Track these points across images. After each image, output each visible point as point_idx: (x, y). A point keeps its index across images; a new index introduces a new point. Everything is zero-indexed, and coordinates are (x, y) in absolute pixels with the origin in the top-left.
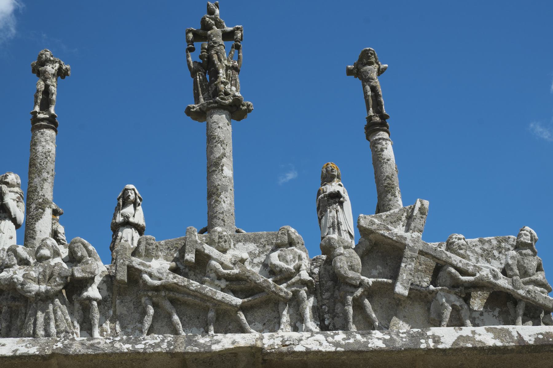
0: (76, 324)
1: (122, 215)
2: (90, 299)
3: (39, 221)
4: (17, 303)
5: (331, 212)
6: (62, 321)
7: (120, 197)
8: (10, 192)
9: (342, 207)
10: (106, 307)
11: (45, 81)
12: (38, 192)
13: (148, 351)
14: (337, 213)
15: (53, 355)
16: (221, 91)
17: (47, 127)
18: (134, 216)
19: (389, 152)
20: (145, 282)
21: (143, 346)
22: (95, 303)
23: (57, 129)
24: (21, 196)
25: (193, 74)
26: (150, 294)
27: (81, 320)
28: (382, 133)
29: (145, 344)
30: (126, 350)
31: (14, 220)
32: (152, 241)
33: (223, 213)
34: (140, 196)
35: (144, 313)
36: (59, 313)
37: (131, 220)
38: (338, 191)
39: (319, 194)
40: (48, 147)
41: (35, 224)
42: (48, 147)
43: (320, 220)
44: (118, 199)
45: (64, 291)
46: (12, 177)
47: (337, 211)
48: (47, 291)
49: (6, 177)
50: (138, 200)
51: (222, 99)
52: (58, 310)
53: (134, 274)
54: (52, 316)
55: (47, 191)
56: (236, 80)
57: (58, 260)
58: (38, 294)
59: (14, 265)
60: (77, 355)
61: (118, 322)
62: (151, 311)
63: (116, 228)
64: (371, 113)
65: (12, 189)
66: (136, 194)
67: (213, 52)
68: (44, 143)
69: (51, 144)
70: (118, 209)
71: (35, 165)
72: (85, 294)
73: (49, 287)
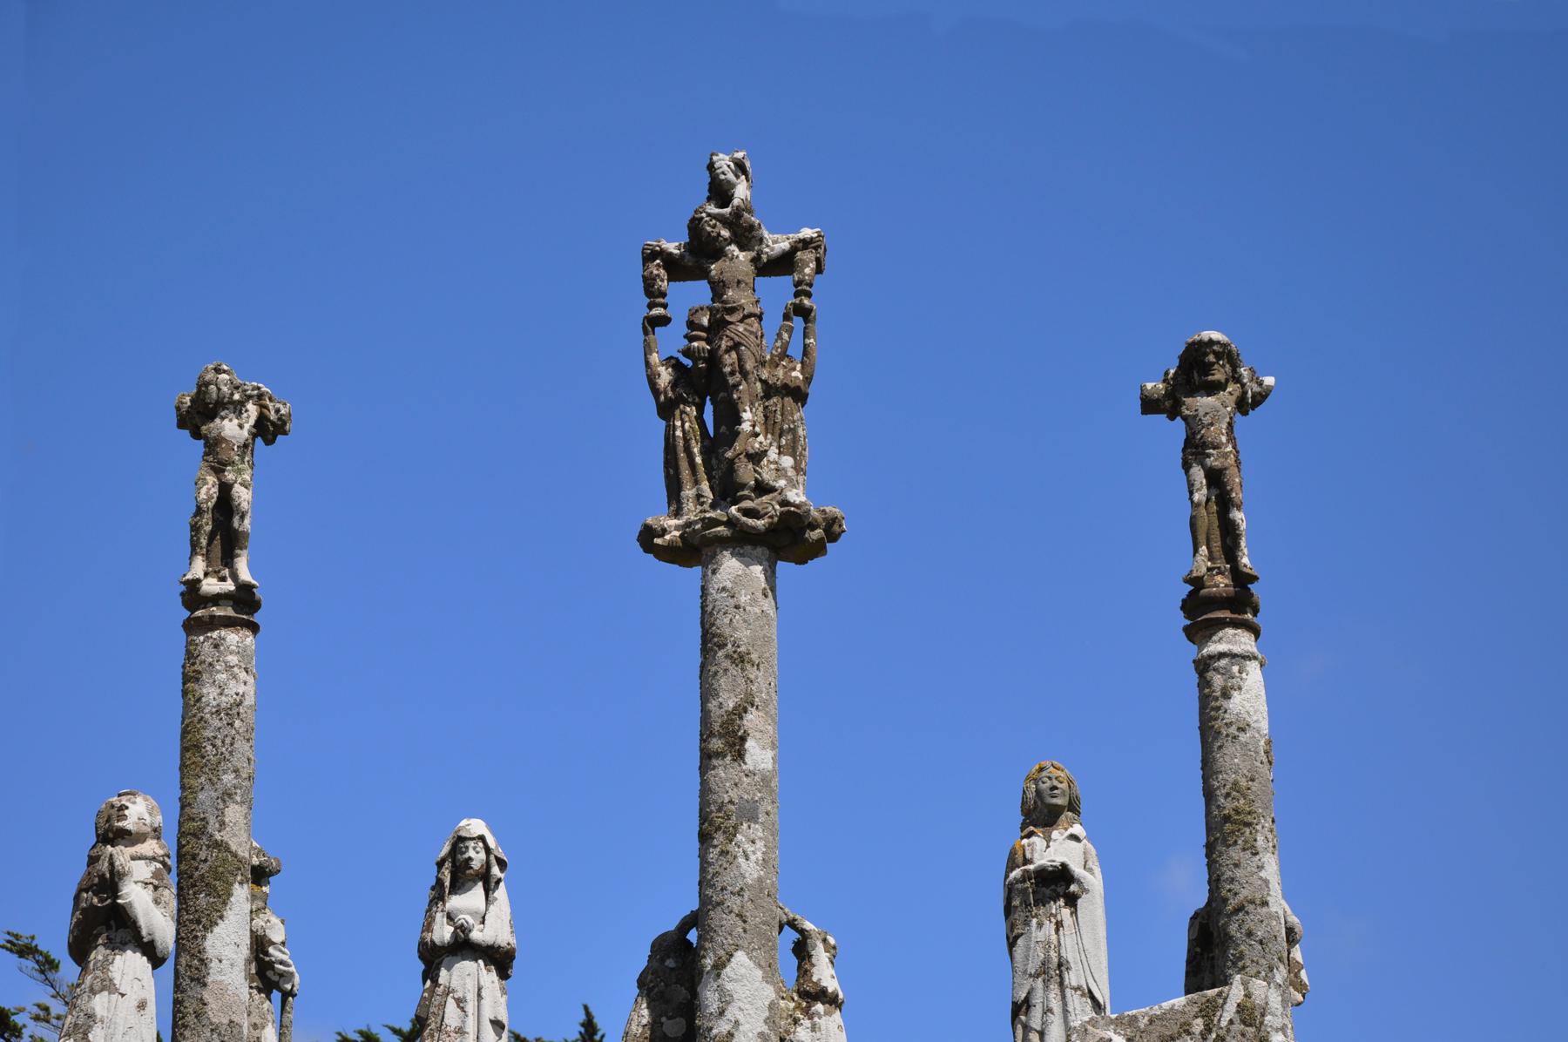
3: (216, 930)
5: (1040, 925)
8: (133, 858)
9: (1074, 913)
11: (218, 470)
14: (1057, 931)
16: (743, 486)
17: (229, 623)
19: (1250, 698)
23: (257, 618)
25: (666, 410)
28: (1230, 631)
33: (740, 893)
37: (476, 935)
38: (1063, 865)
39: (1012, 865)
40: (234, 688)
41: (204, 937)
43: (1012, 944)
47: (1059, 925)
50: (495, 870)
51: (748, 513)
56: (793, 431)
63: (433, 958)
64: (1202, 564)
66: (488, 850)
67: (724, 344)
68: (222, 677)
69: (243, 675)
71: (197, 747)
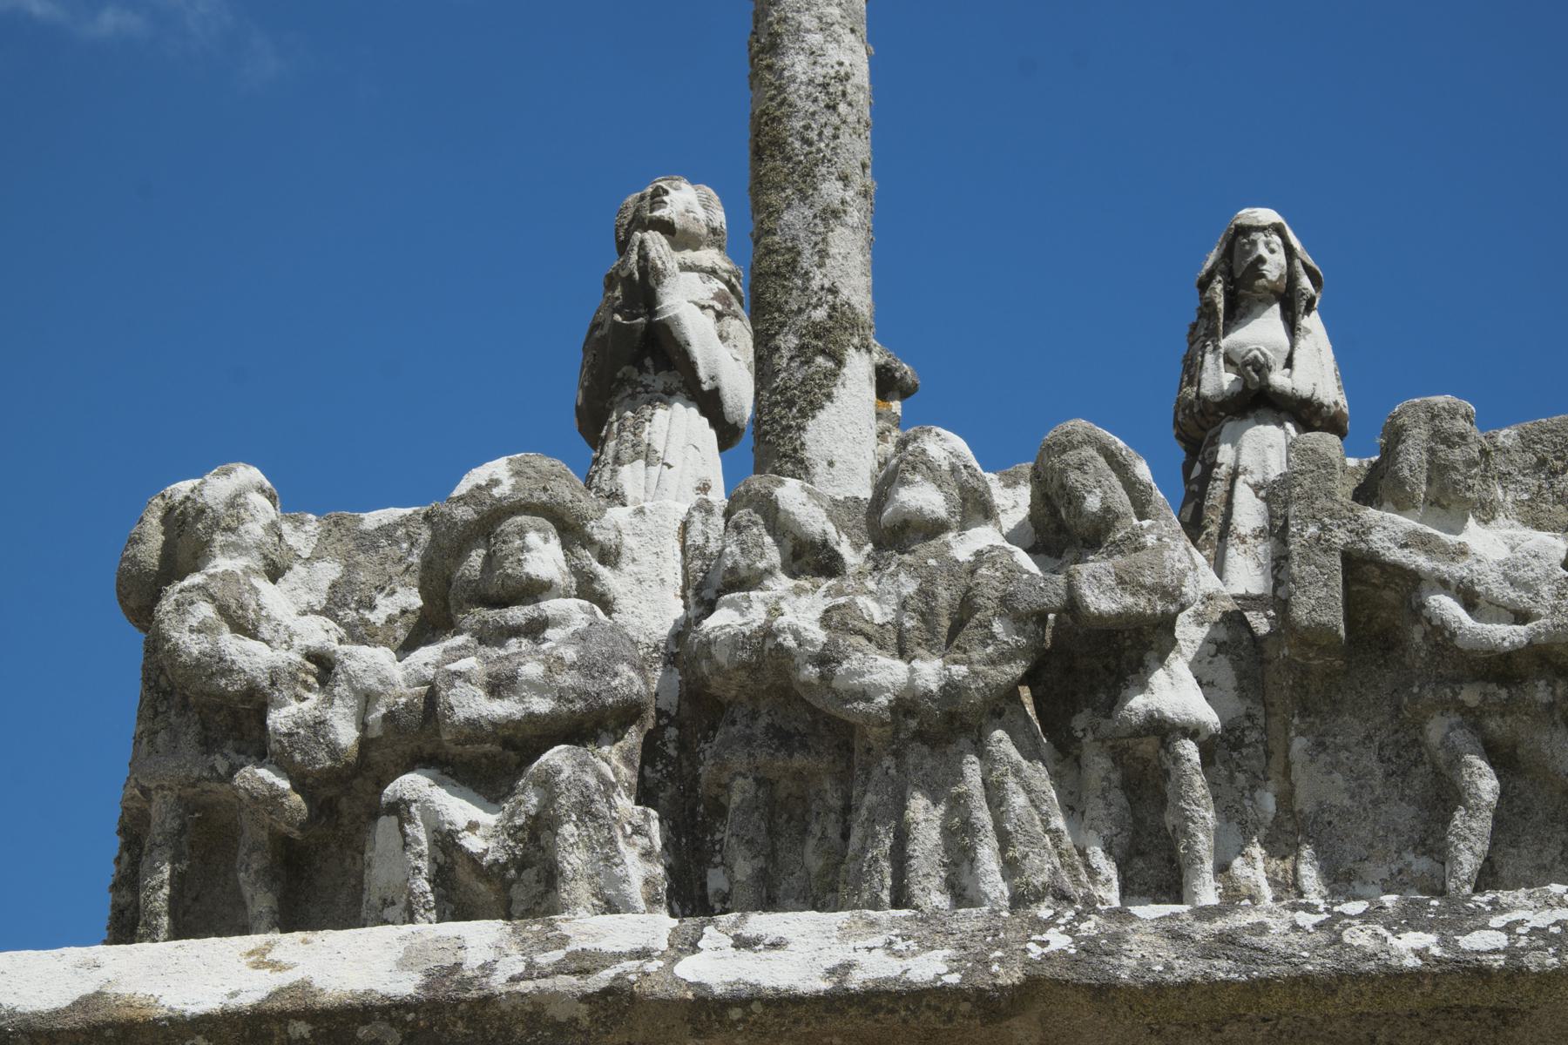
0: (1098, 857)
1: (1229, 361)
2: (1162, 730)
3: (822, 415)
4: (799, 761)
6: (1033, 841)
7: (1211, 275)
10: (1241, 778)
12: (806, 276)
13: (1532, 962)
15: (1034, 987)
18: (1289, 363)
20: (1441, 633)
21: (1502, 940)
22: (1189, 750)
24: (732, 288)
26: (1470, 695)
27: (1123, 839)
29: (1509, 929)
30: (1411, 962)
31: (710, 404)
32: (1461, 425)
34: (1310, 261)
35: (1446, 796)
36: (1019, 800)
37: (1279, 379)
40: (834, 54)
41: (801, 428)
42: (834, 54)
44: (1204, 285)
45: (1025, 693)
46: (685, 201)
48: (951, 689)
49: (658, 197)
50: (1305, 282)
52: (1011, 783)
53: (1381, 597)
54: (983, 816)
55: (846, 268)
57: (983, 537)
58: (907, 705)
59: (769, 572)
60: (1158, 989)
61: (1307, 851)
62: (1486, 784)
65: (689, 256)
68: (815, 39)
69: (849, 39)
70: (1207, 327)
71: (779, 144)
72: (1138, 703)
73: (960, 671)
